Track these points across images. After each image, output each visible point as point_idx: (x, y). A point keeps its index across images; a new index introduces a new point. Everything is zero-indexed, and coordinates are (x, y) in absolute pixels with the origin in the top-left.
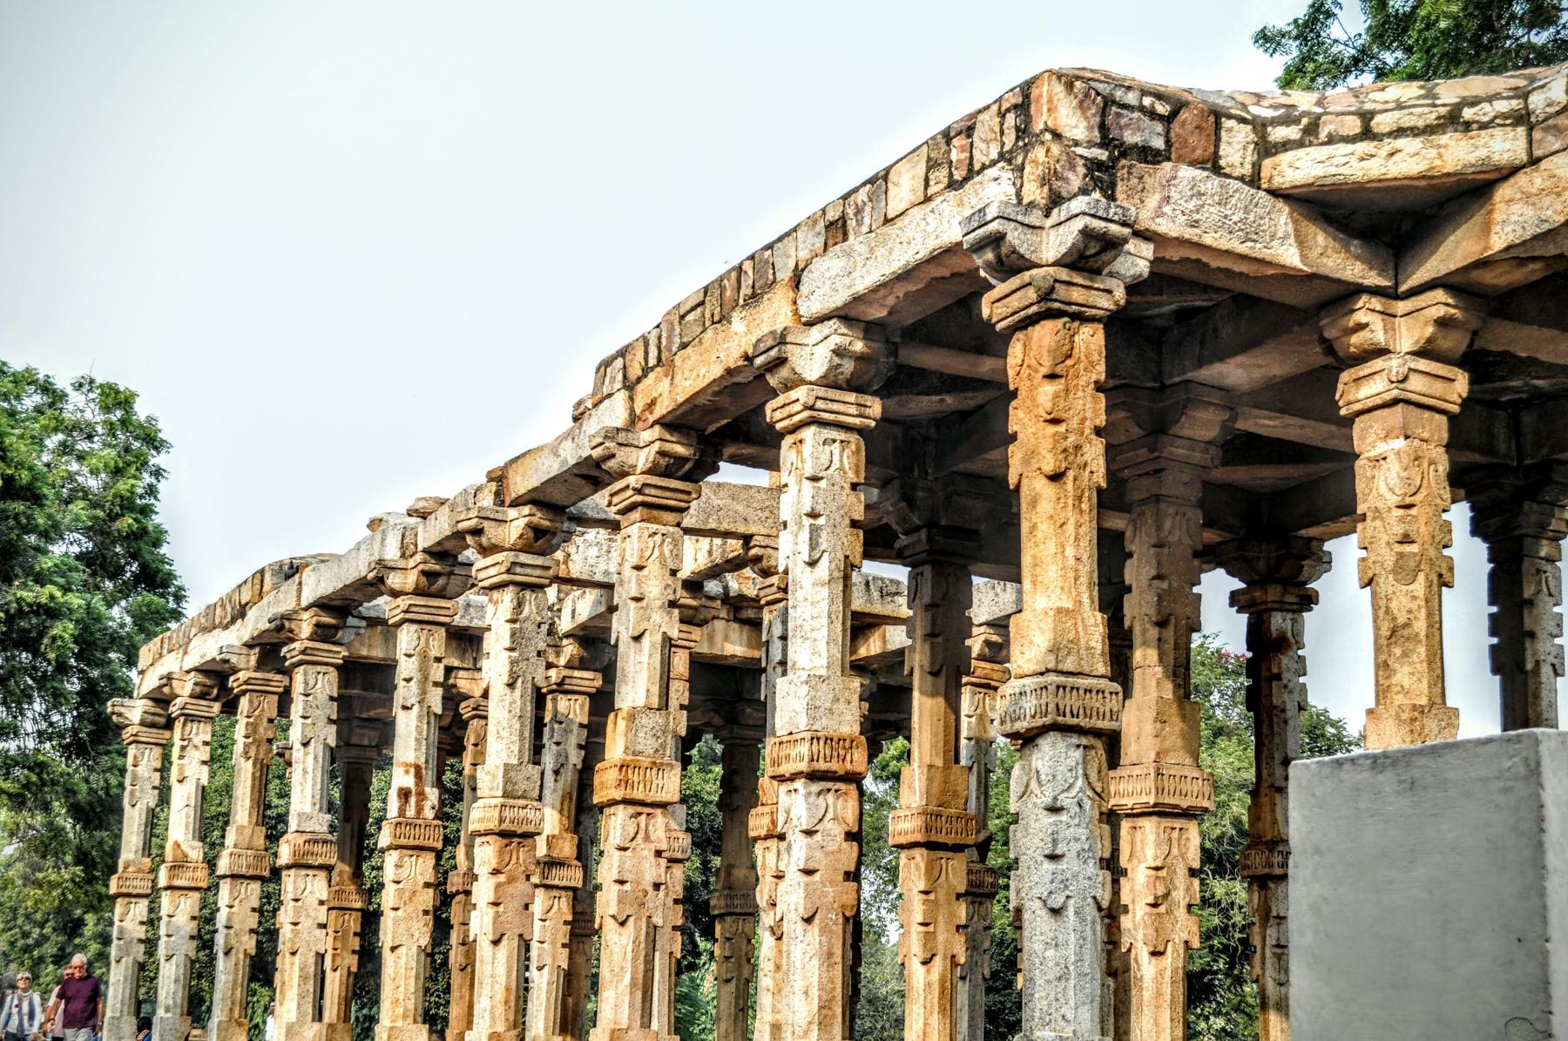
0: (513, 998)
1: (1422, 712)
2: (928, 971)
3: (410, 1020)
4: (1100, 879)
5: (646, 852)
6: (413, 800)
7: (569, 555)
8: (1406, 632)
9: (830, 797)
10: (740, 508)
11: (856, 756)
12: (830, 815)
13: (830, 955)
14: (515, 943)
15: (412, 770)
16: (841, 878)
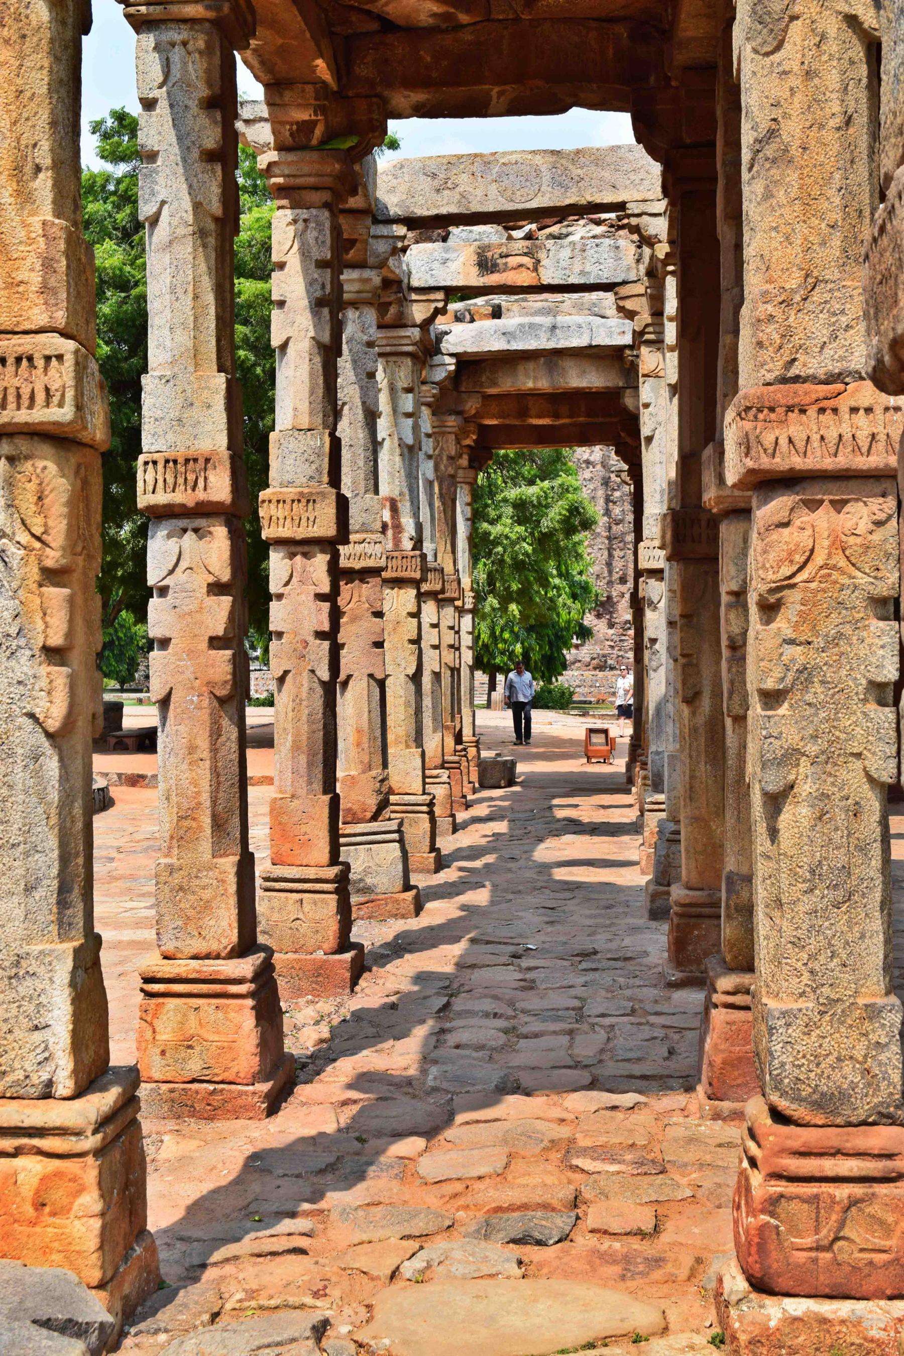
0: (365, 740)
1: (787, 303)
2: (693, 713)
3: (402, 746)
4: (43, 683)
5: (303, 597)
6: (390, 533)
7: (539, 261)
8: (769, 151)
9: (190, 537)
10: (606, 174)
11: (212, 478)
12: (183, 564)
13: (192, 749)
14: (364, 683)
15: (388, 504)
16: (205, 645)
